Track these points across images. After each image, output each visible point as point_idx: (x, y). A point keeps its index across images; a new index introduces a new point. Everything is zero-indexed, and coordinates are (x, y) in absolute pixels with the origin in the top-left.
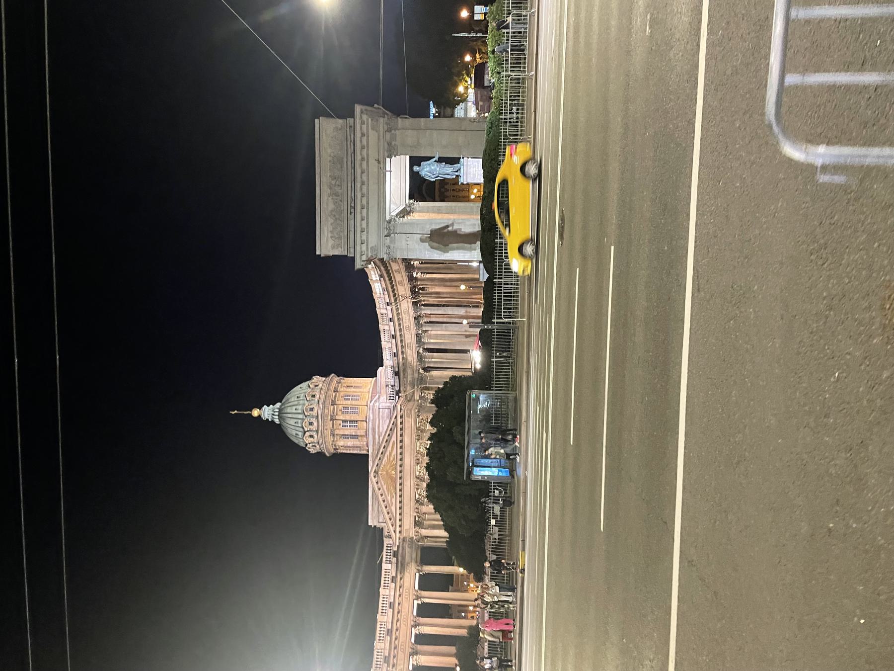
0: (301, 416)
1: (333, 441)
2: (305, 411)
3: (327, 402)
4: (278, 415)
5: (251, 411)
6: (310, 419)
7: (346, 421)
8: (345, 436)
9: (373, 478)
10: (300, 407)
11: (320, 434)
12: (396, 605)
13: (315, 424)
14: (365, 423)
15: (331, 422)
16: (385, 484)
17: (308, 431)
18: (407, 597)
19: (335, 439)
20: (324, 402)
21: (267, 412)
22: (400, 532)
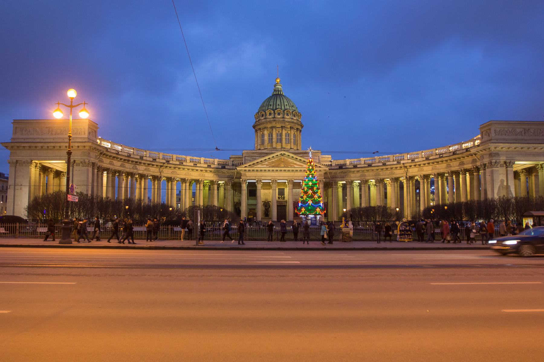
0: (283, 108)
1: (267, 128)
2: (287, 110)
3: (292, 124)
4: (274, 94)
6: (282, 113)
7: (281, 135)
8: (271, 135)
9: (281, 153)
10: (288, 107)
11: (273, 120)
12: (197, 168)
14: (280, 147)
15: (280, 126)
16: (275, 160)
18: (200, 175)
19: (268, 129)
22: (245, 170)
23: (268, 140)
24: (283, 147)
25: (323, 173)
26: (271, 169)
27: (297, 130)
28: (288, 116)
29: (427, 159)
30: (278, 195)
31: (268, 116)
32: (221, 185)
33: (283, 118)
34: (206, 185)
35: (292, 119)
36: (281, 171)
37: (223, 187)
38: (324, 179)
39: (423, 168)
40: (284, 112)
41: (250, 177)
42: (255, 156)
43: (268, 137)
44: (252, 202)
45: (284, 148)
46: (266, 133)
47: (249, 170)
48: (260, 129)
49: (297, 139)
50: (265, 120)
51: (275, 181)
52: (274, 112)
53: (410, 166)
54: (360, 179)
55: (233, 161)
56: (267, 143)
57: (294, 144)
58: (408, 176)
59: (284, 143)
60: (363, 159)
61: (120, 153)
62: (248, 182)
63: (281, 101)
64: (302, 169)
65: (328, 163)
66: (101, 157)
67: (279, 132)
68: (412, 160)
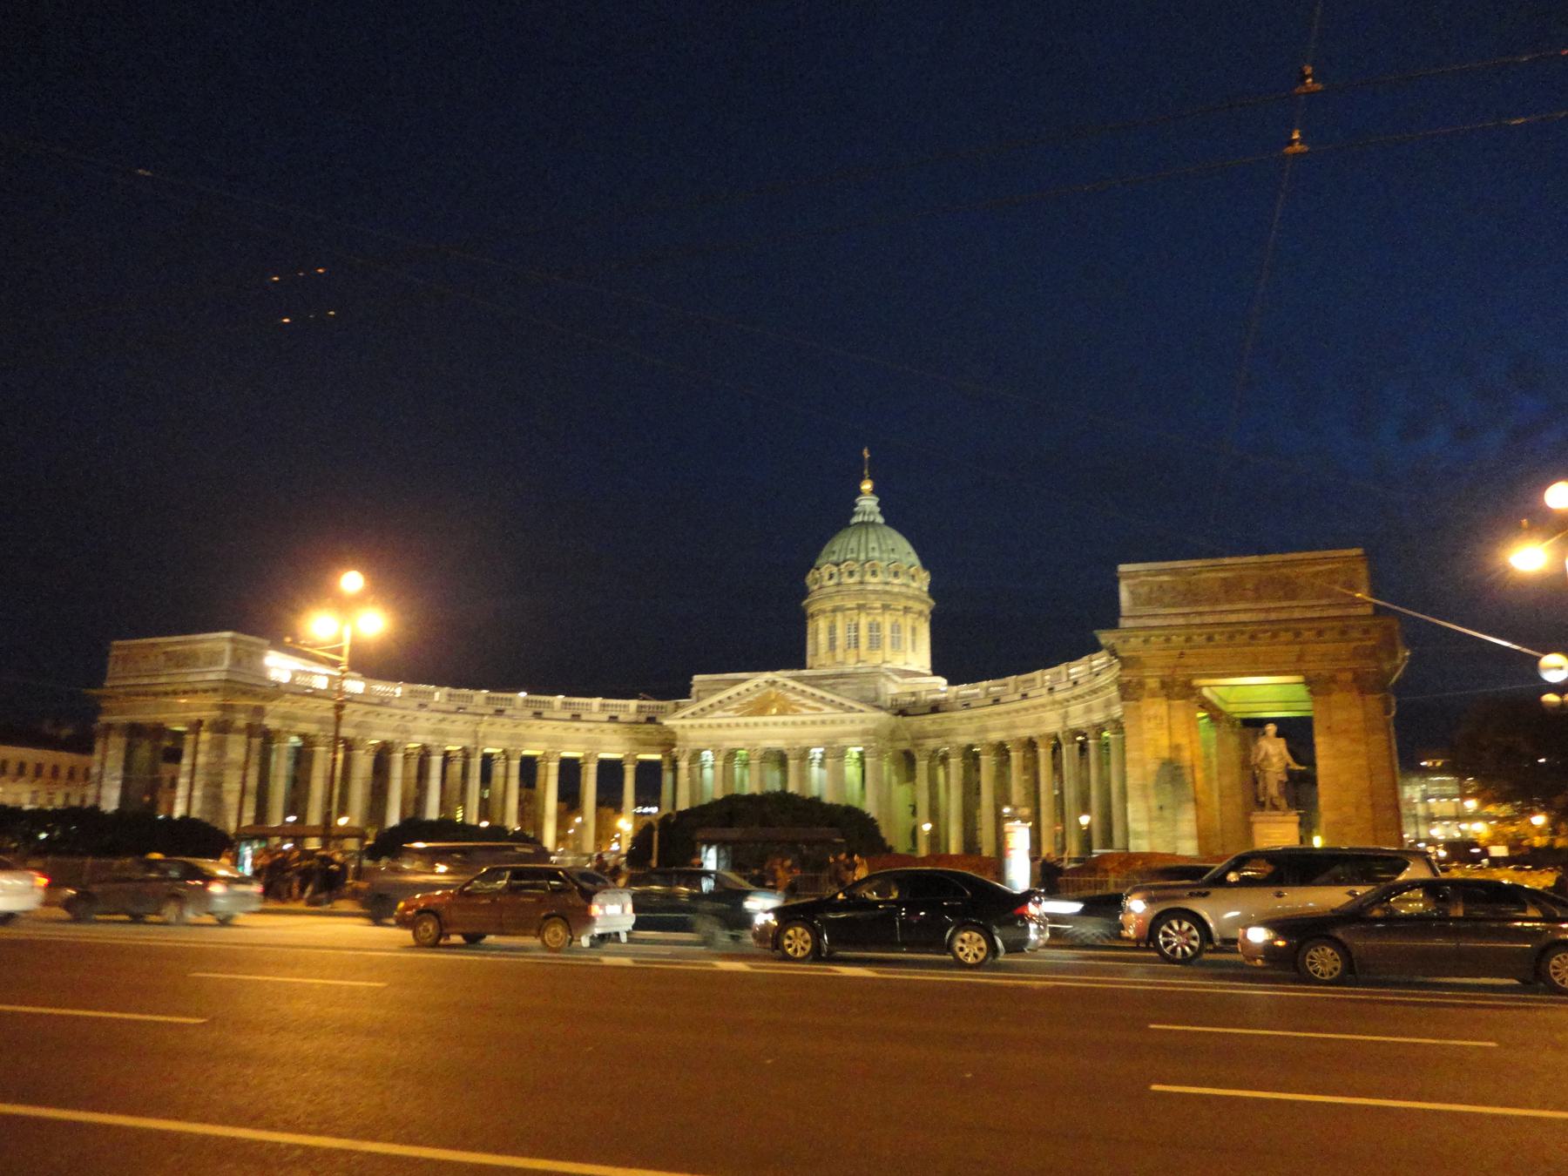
0: (862, 557)
2: (871, 562)
3: (887, 597)
5: (870, 478)
7: (857, 628)
8: (832, 630)
10: (876, 554)
13: (851, 581)
17: (839, 570)
20: (886, 592)
21: (868, 503)
22: (683, 727)
24: (862, 659)
26: (742, 720)
33: (861, 583)
35: (887, 583)
36: (766, 724)
40: (863, 569)
43: (827, 634)
45: (864, 661)
56: (824, 651)
63: (860, 541)
64: (818, 718)
67: (851, 620)
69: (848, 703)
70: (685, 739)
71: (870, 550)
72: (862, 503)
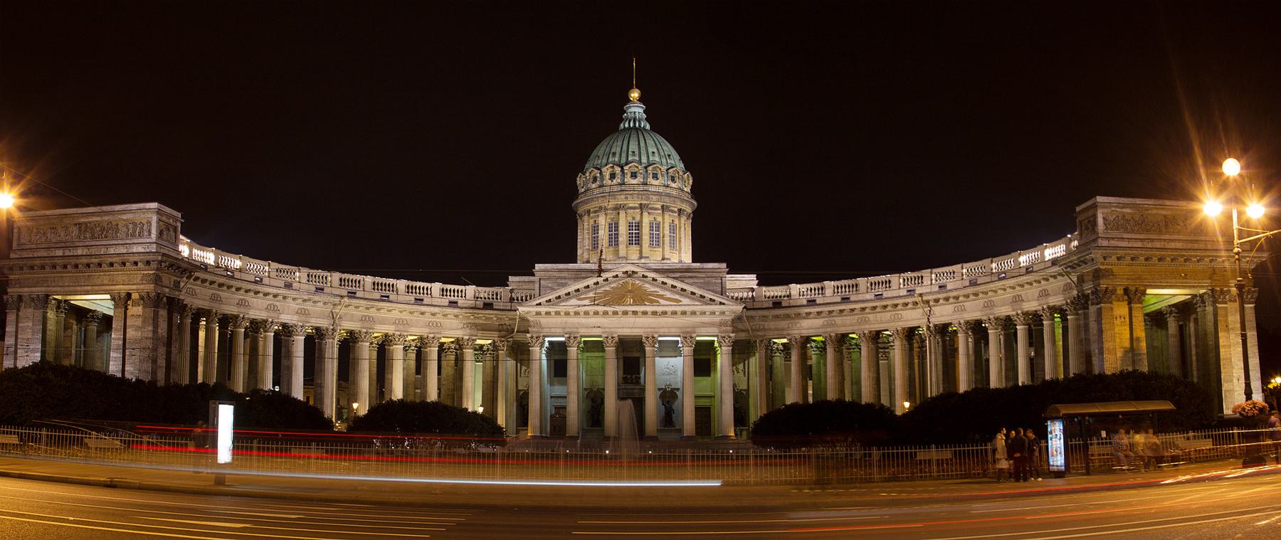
0: (644, 160)
1: (606, 209)
2: (655, 166)
3: (667, 199)
5: (636, 88)
6: (641, 173)
7: (639, 226)
8: (614, 227)
10: (657, 159)
15: (637, 205)
16: (612, 288)
21: (636, 110)
22: (538, 314)
23: (607, 238)
25: (729, 318)
26: (601, 309)
27: (679, 215)
28: (658, 179)
29: (973, 283)
30: (624, 374)
31: (607, 181)
32: (485, 348)
34: (449, 349)
36: (625, 313)
37: (490, 354)
38: (732, 333)
39: (964, 304)
40: (647, 171)
41: (550, 328)
42: (565, 278)
44: (558, 390)
46: (602, 221)
47: (548, 313)
48: (589, 212)
49: (680, 235)
50: (601, 190)
51: (612, 338)
52: (622, 170)
53: (937, 301)
54: (824, 333)
55: (512, 291)
57: (672, 246)
58: (931, 325)
59: (648, 244)
60: (829, 285)
61: (237, 275)
62: (550, 343)
63: (639, 144)
64: (679, 309)
65: (745, 295)
66: (189, 286)
67: (634, 218)
68: (940, 287)
69: (709, 295)
70: (539, 325)
71: (650, 154)
72: (632, 110)
